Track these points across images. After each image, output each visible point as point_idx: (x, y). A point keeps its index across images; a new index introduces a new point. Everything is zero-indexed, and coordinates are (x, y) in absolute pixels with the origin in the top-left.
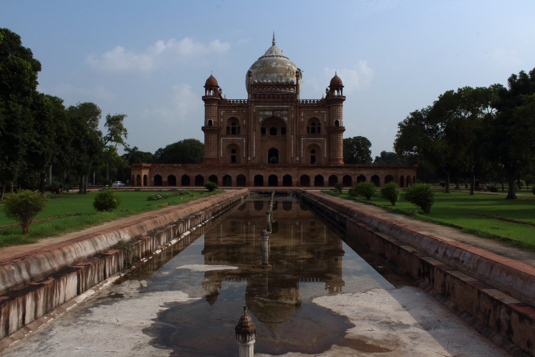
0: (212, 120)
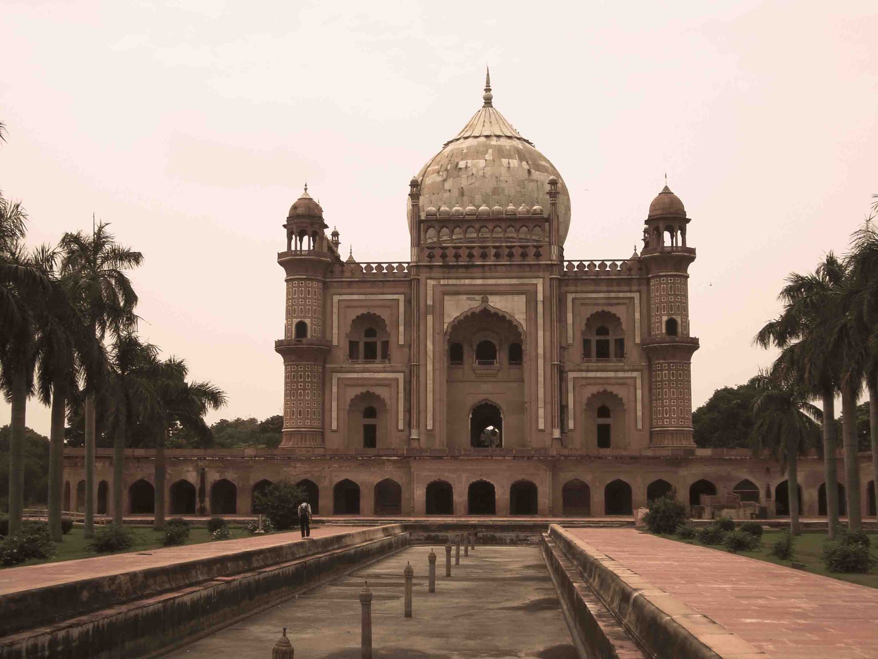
0: (308, 321)
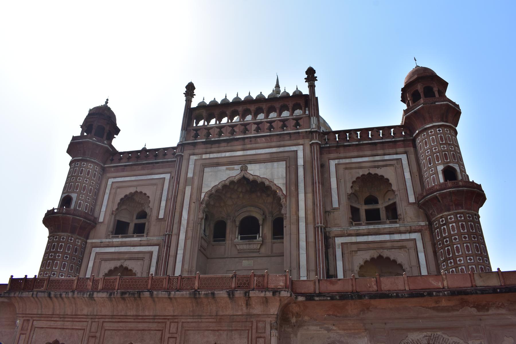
0: (74, 196)
